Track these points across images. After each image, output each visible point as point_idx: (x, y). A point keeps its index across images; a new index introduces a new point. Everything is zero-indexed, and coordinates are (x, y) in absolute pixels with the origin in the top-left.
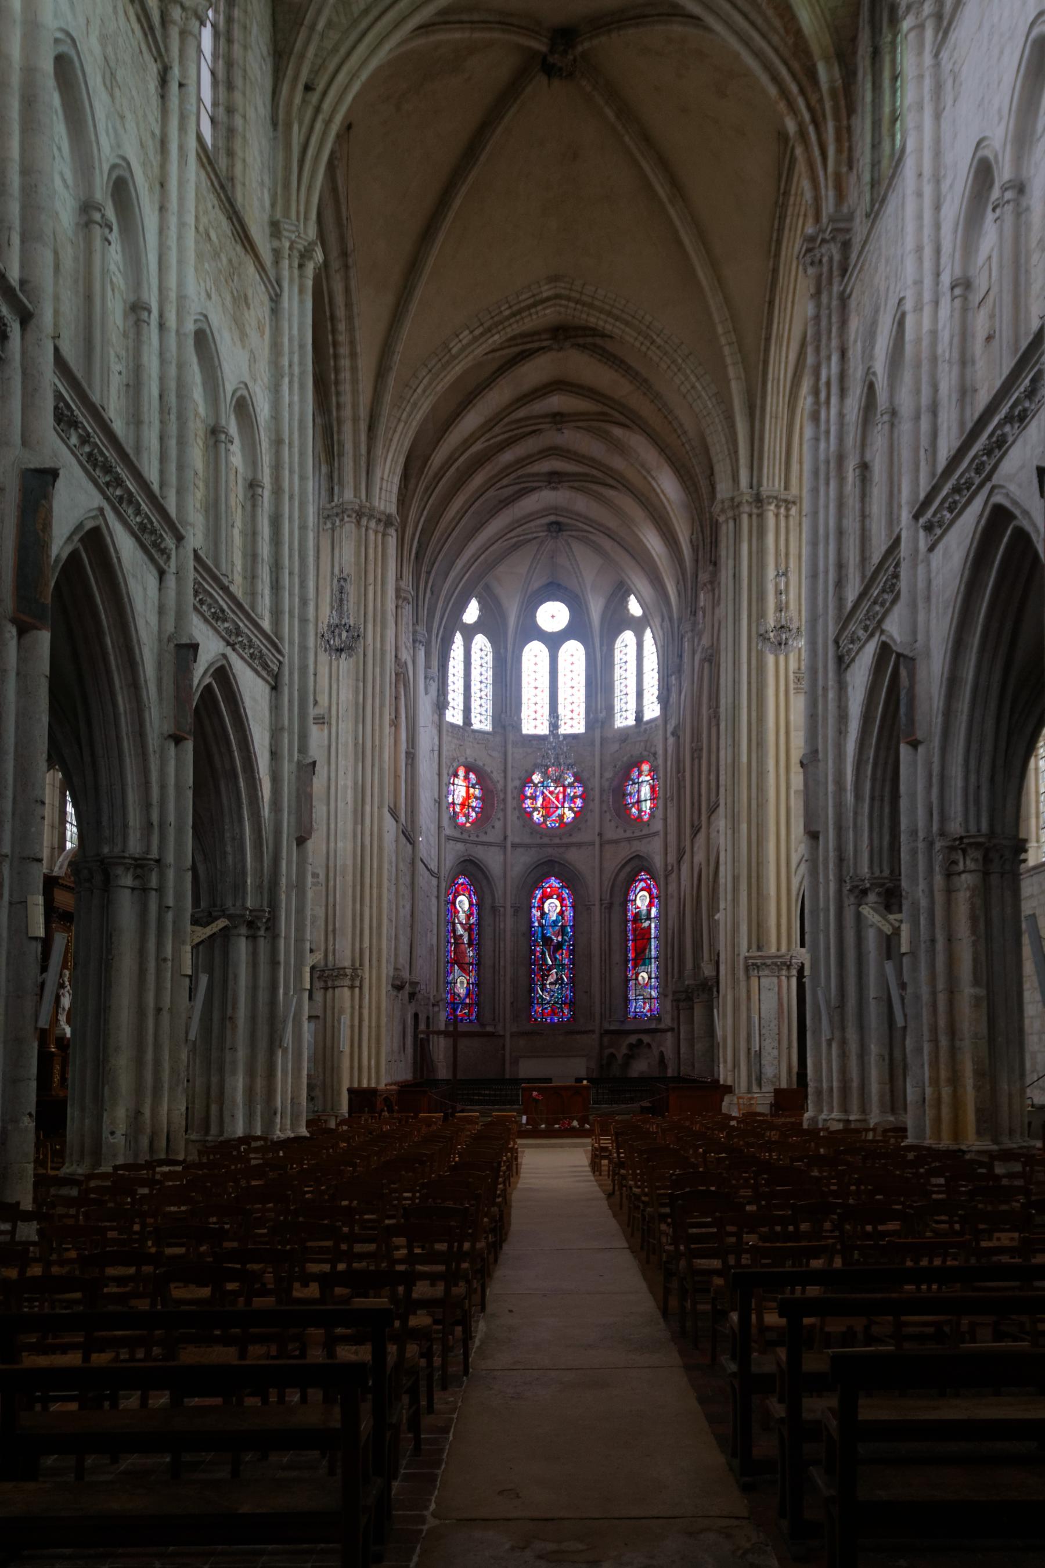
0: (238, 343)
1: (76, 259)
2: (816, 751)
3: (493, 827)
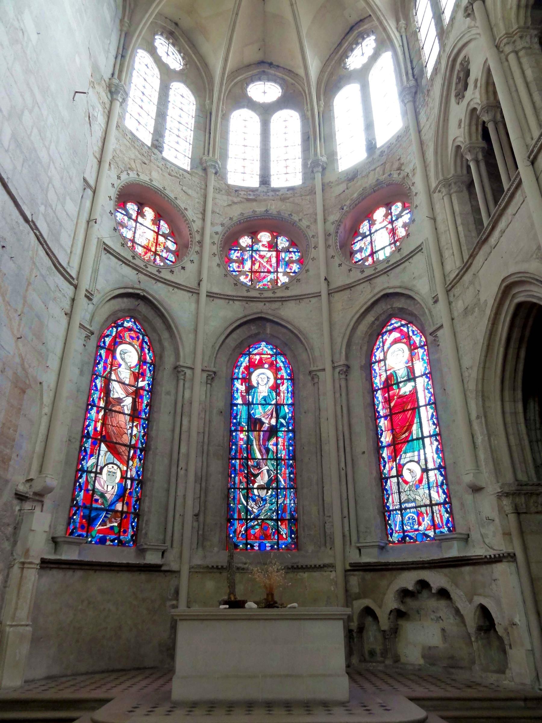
3: (183, 268)
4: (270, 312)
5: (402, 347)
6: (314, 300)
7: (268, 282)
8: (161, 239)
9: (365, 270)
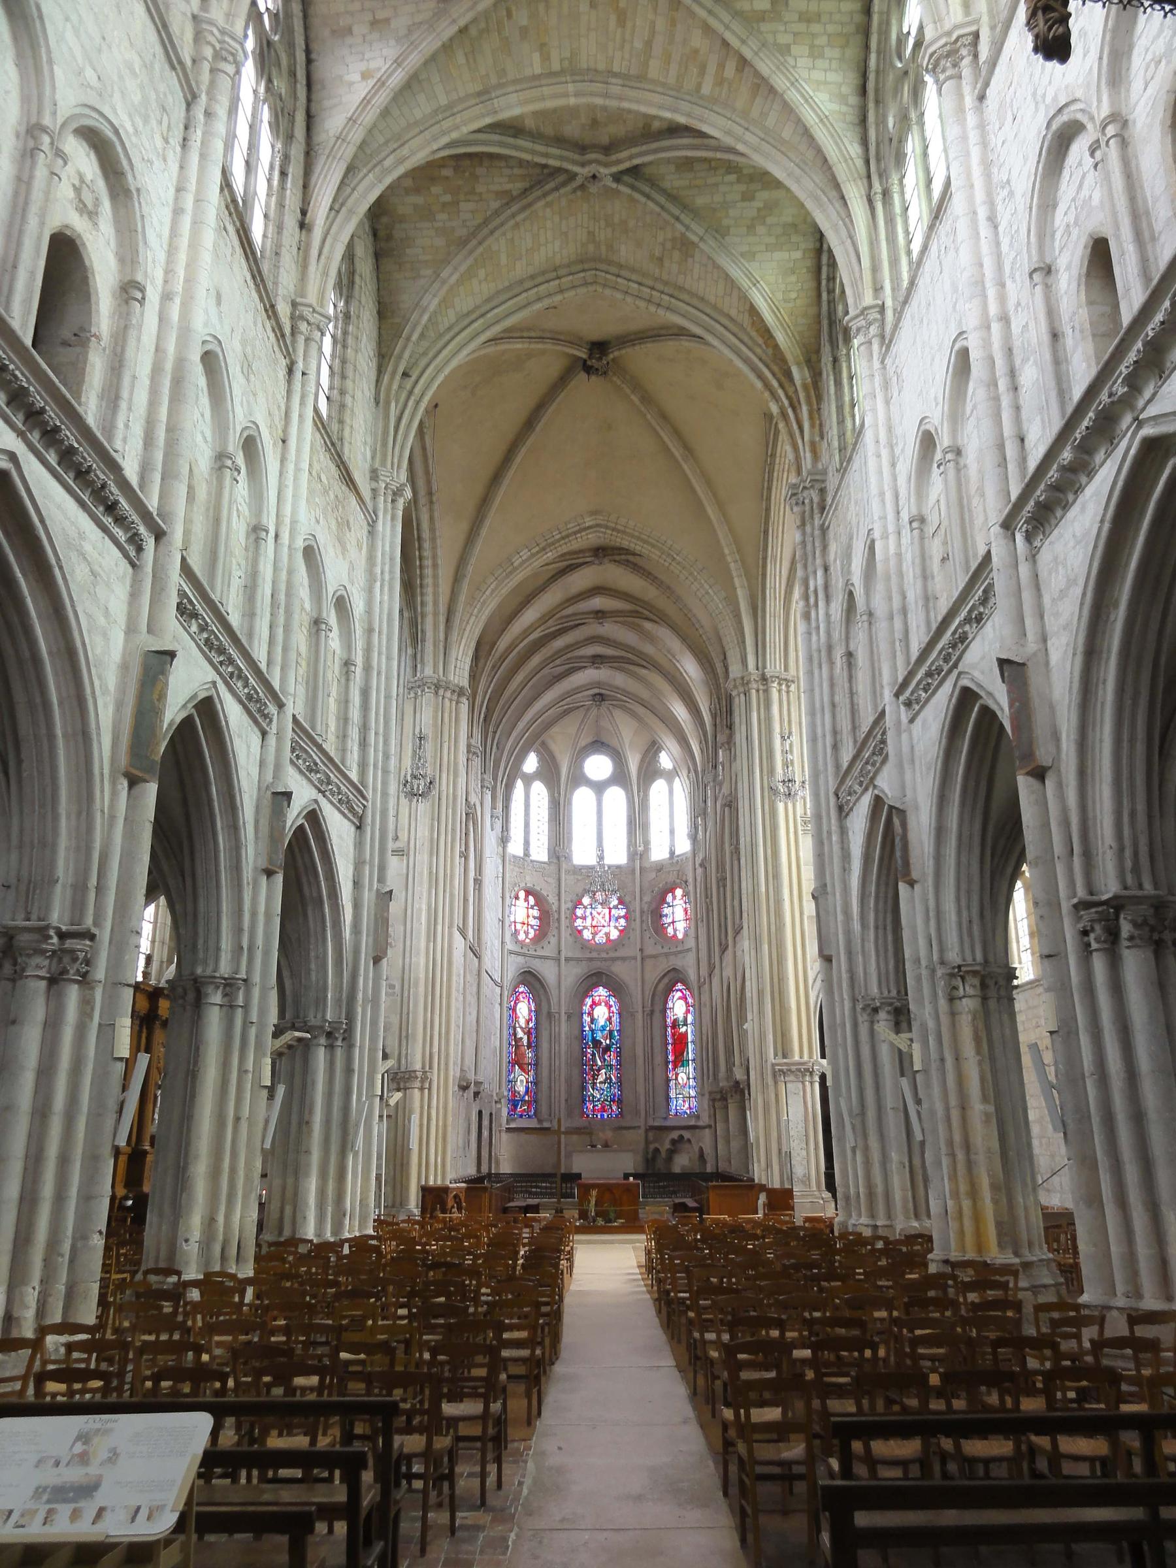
0: (341, 556)
1: (209, 494)
2: (825, 885)
5: (682, 1002)
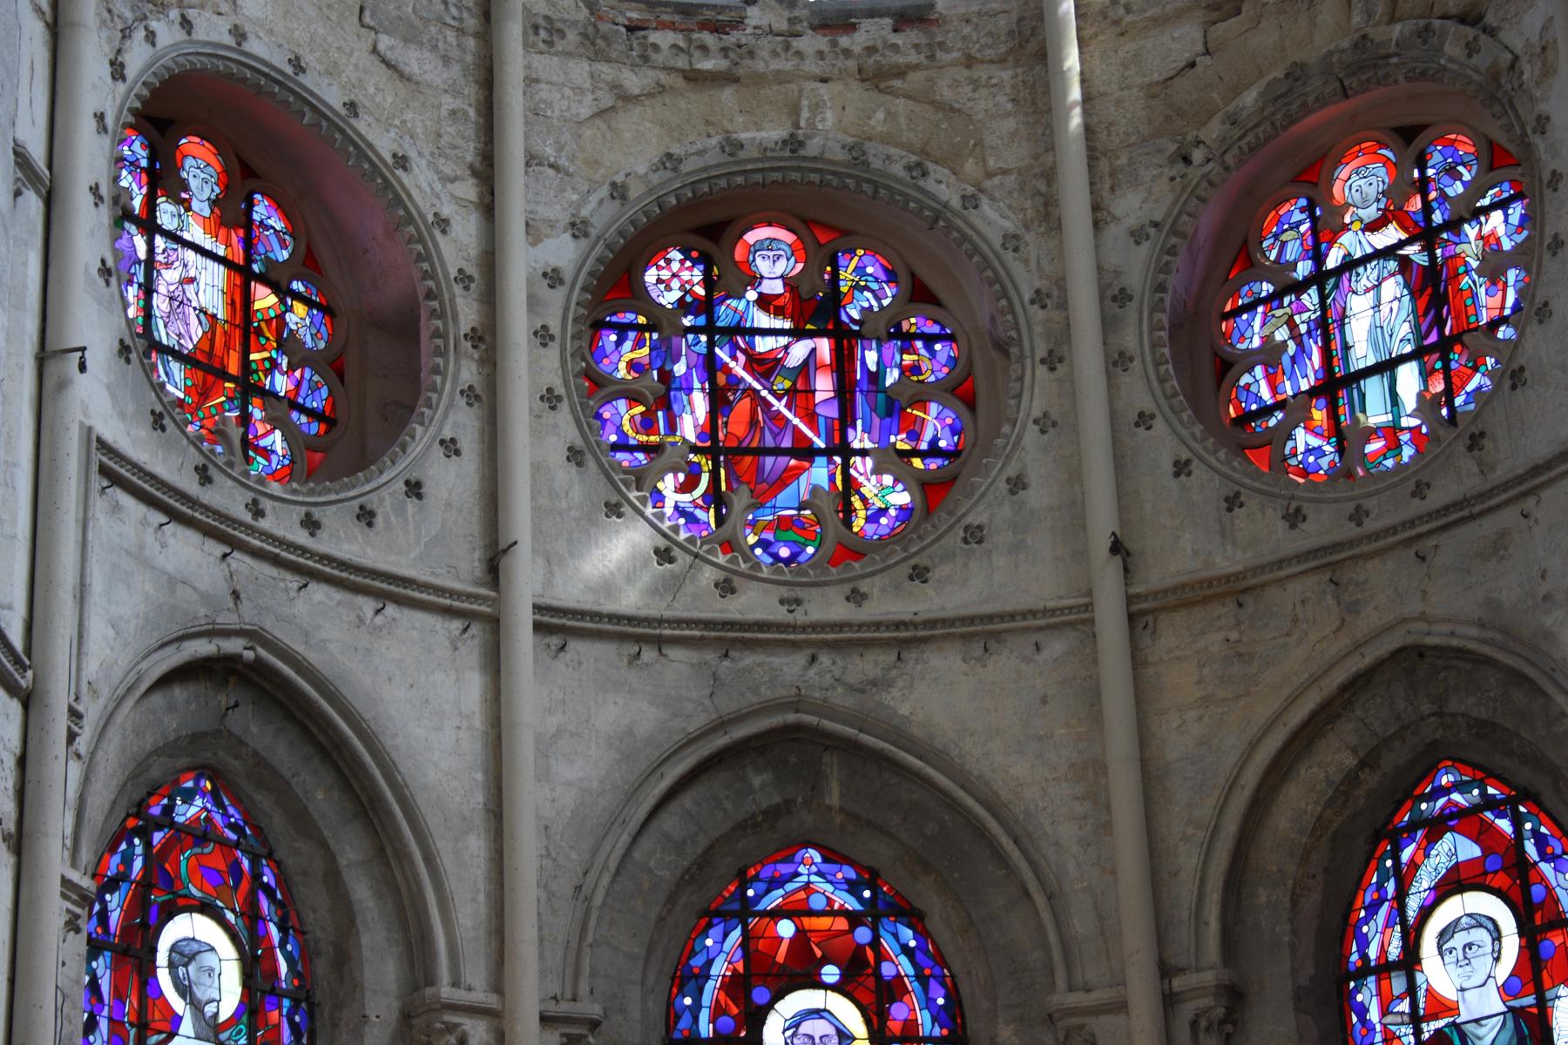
3: (414, 489)
4: (839, 698)
6: (1056, 647)
7: (801, 507)
8: (265, 300)
9: (1308, 509)
